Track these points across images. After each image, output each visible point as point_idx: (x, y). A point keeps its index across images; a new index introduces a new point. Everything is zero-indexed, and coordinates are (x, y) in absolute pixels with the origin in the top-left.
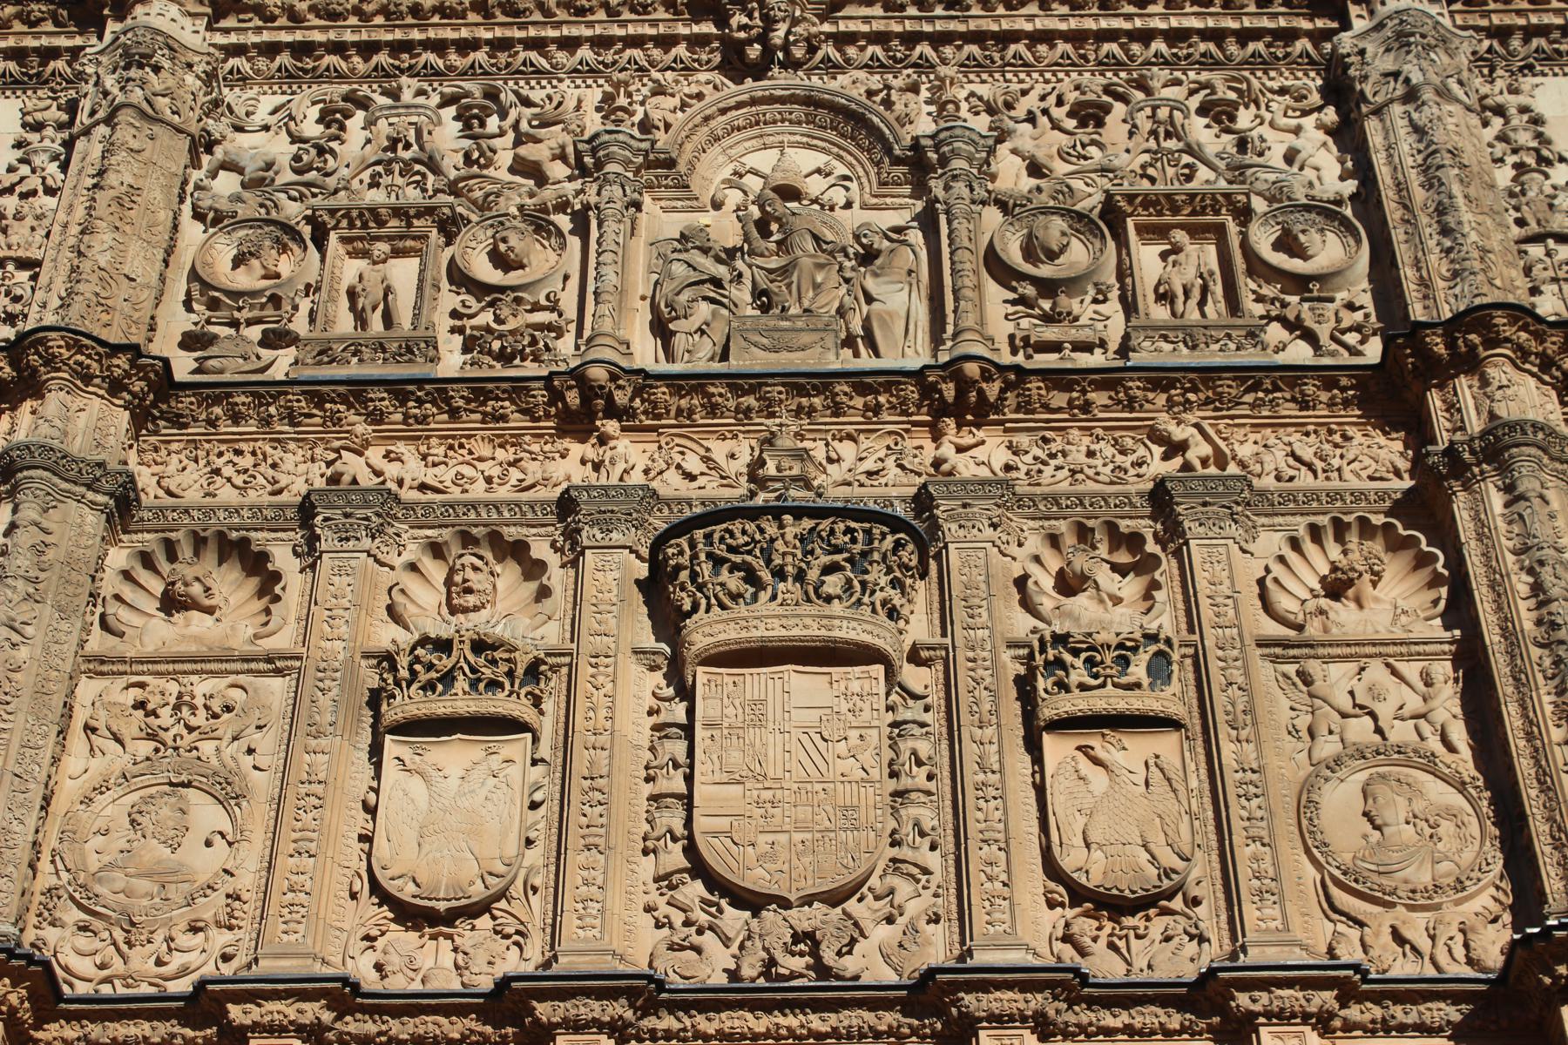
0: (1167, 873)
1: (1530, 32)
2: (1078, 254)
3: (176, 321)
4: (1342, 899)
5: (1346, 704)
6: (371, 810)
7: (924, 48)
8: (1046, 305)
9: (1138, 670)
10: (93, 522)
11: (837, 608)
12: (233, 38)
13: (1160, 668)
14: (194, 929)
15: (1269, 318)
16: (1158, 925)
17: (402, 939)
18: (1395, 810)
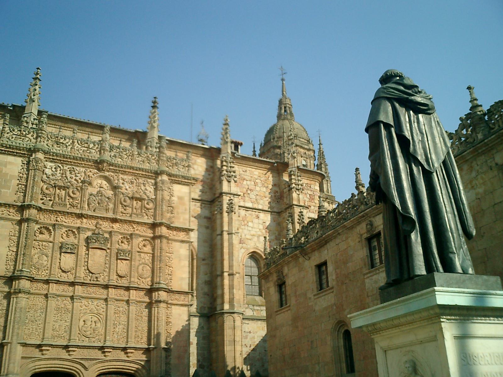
0: (126, 274)
1: (175, 180)
2: (128, 201)
3: (40, 197)
4: (139, 278)
5: (143, 258)
6: (60, 260)
7: (118, 171)
8: (125, 208)
9: (127, 255)
10: (34, 224)
11: (103, 245)
12: (47, 156)
14: (44, 270)
15: (144, 212)
16: (124, 278)
17: (64, 274)
18: (144, 269)
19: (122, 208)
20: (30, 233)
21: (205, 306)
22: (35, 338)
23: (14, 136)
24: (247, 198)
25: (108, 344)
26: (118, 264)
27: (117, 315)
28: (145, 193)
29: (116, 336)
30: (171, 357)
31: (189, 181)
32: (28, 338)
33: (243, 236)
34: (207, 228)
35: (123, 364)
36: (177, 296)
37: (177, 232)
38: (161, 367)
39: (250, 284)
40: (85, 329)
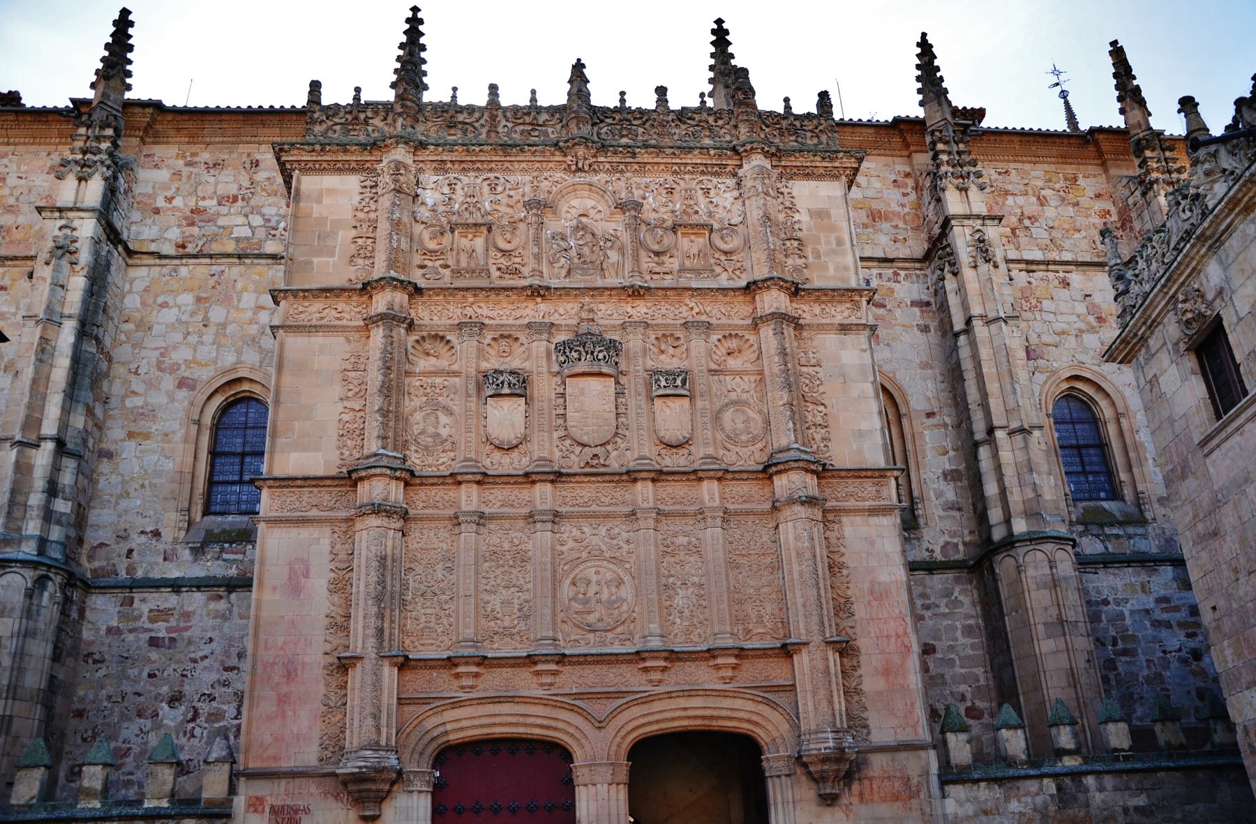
0: (684, 437)
5: (730, 388)
7: (622, 167)
8: (656, 259)
9: (679, 382)
10: (403, 331)
12: (421, 159)
13: (684, 382)
16: (681, 452)
17: (497, 455)
19: (649, 260)
20: (391, 354)
21: (955, 540)
22: (438, 643)
23: (337, 128)
24: (1023, 240)
25: (655, 643)
26: (657, 413)
27: (672, 560)
28: (710, 214)
29: (678, 621)
30: (859, 672)
31: (837, 164)
32: (416, 643)
33: (1034, 339)
34: (925, 329)
35: (711, 702)
36: (852, 485)
37: (823, 306)
38: (831, 702)
39: (1079, 469)
40: (577, 606)
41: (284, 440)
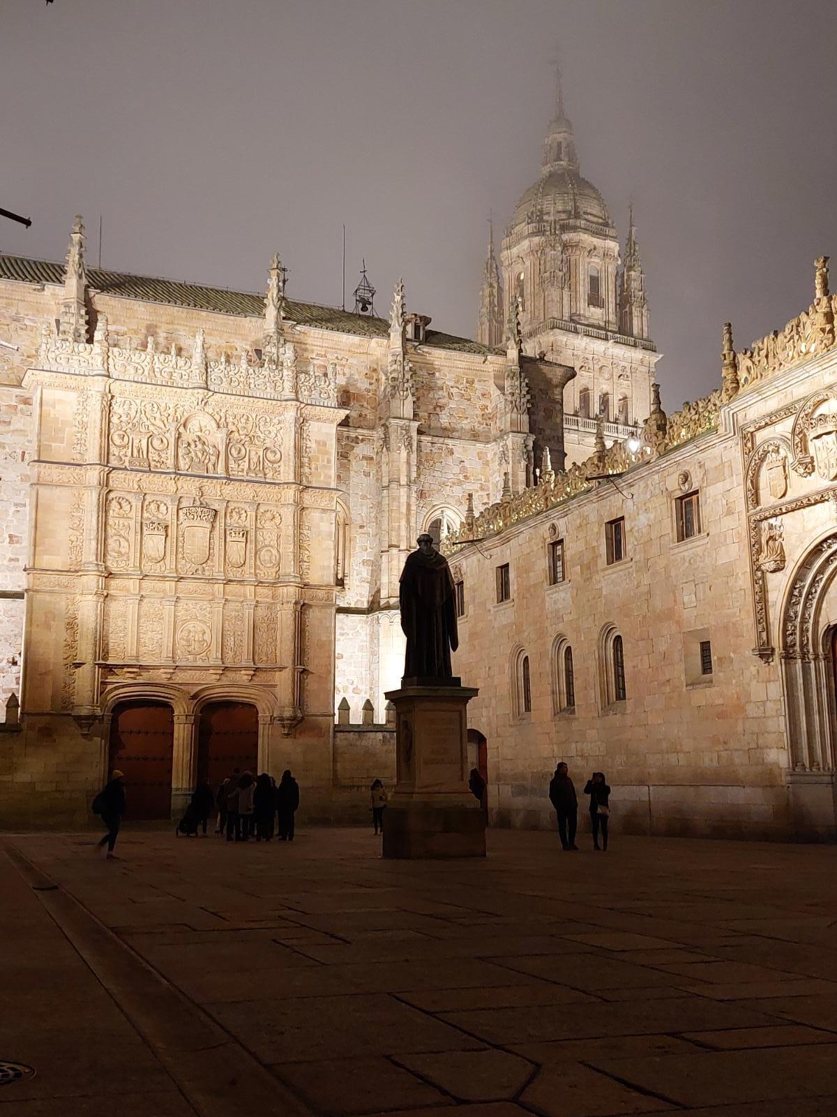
13: (243, 534)
21: (363, 599)
29: (230, 652)
35: (240, 690)
41: (41, 548)
